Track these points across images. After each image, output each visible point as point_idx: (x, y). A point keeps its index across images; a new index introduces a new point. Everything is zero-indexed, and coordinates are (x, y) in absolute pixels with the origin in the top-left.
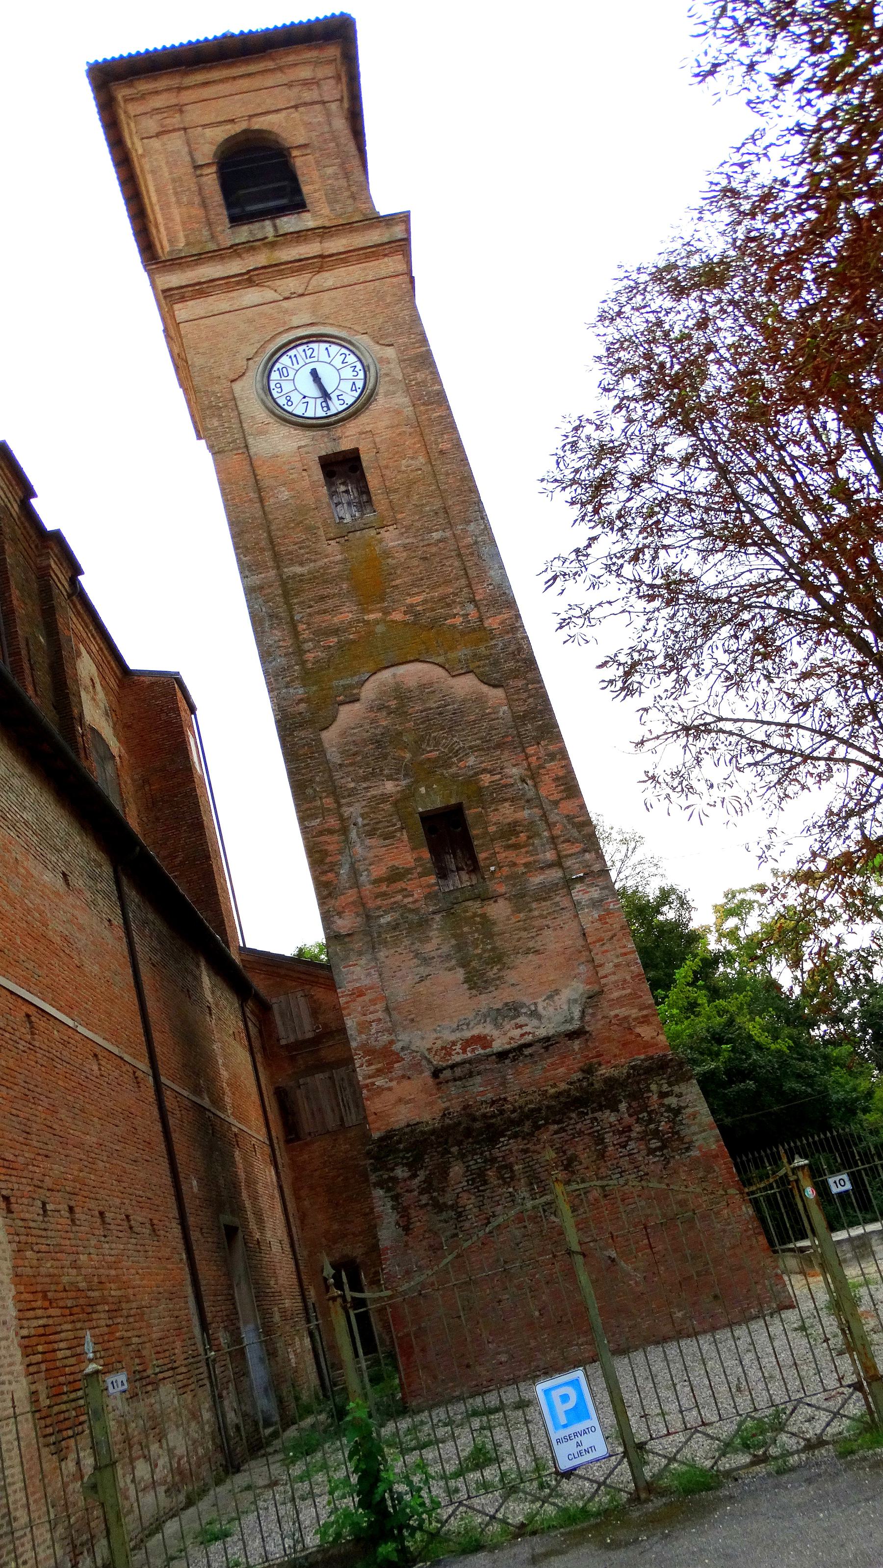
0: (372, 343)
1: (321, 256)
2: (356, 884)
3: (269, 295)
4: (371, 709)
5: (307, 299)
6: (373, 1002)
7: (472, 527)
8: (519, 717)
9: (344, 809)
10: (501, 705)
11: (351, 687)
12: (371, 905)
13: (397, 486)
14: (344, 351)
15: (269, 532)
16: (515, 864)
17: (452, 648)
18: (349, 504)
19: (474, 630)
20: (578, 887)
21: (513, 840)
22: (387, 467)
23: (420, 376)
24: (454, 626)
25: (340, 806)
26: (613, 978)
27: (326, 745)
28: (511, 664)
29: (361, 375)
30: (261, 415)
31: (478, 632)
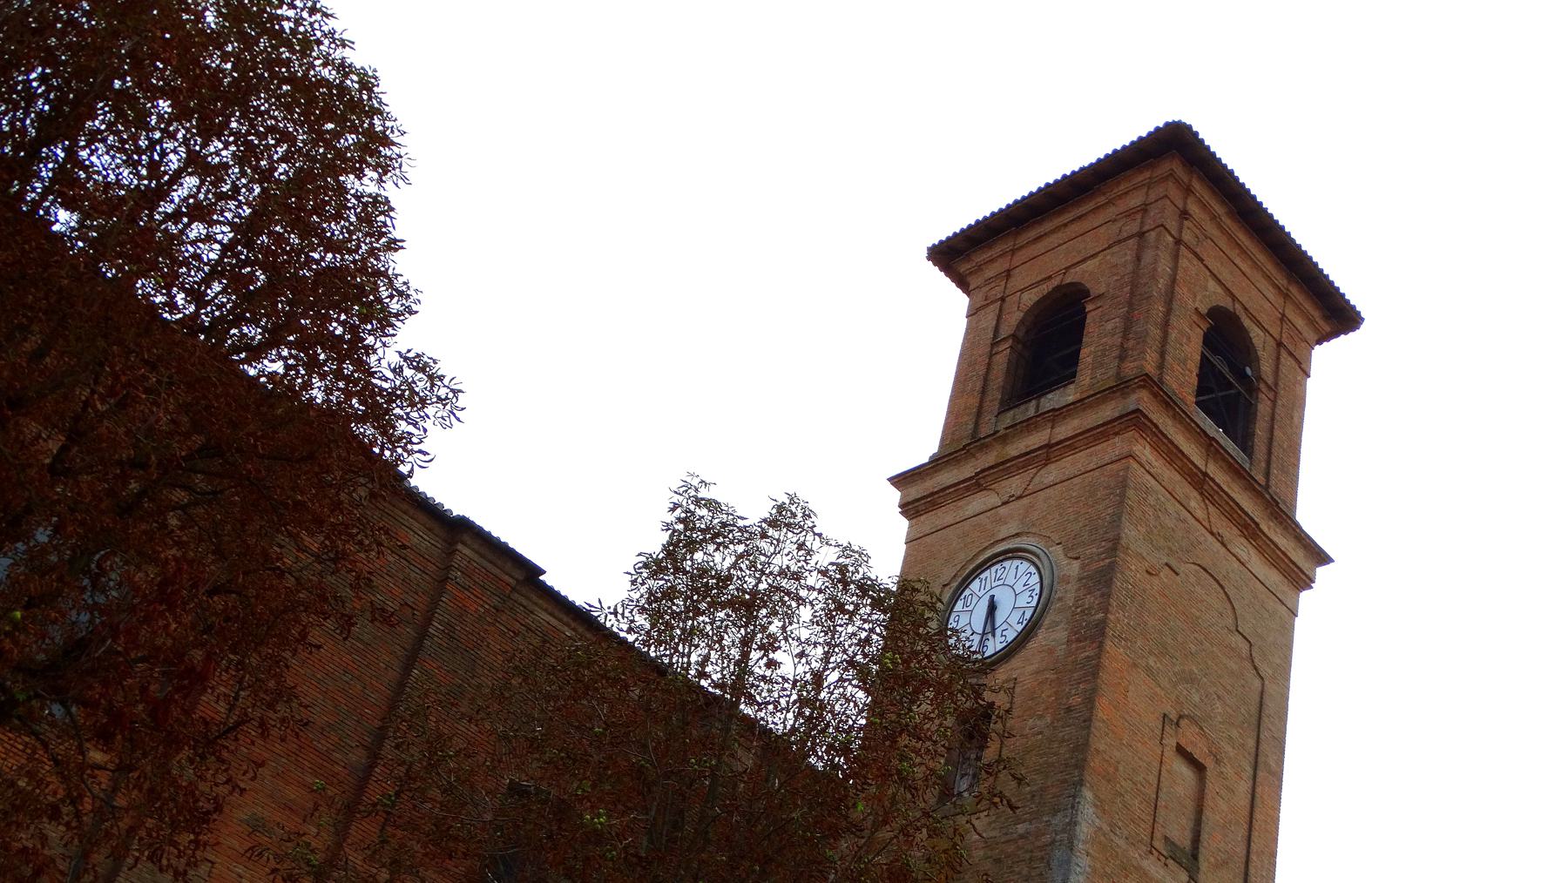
1: (1048, 446)
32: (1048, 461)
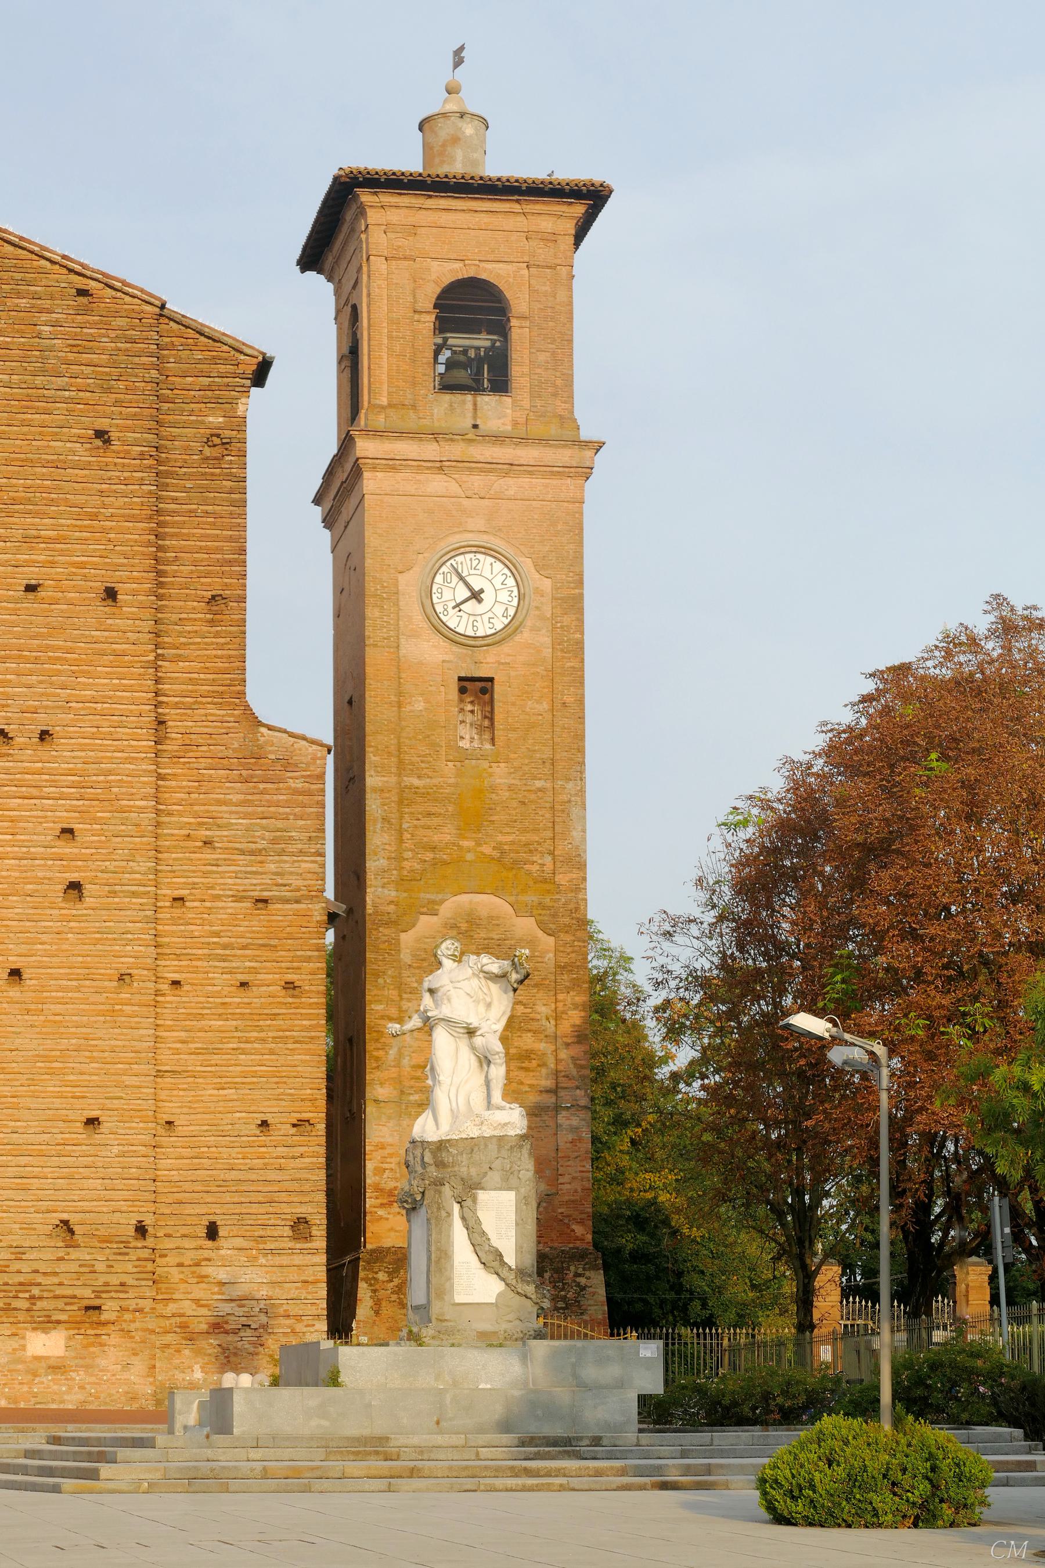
0: (533, 570)
2: (398, 1065)
3: (454, 488)
4: (445, 925)
5: (486, 502)
6: (391, 1155)
7: (570, 785)
8: (560, 967)
9: (403, 1002)
10: (548, 951)
11: (434, 902)
12: (407, 1083)
13: (517, 725)
14: (506, 571)
15: (399, 738)
16: (522, 1083)
17: (524, 891)
18: (471, 725)
19: (545, 881)
20: (564, 1113)
21: (526, 1064)
22: (513, 704)
23: (567, 620)
24: (529, 873)
25: (402, 999)
26: (568, 1186)
27: (402, 946)
28: (567, 920)
29: (515, 603)
30: (418, 617)
31: (547, 882)
32: (506, 474)
